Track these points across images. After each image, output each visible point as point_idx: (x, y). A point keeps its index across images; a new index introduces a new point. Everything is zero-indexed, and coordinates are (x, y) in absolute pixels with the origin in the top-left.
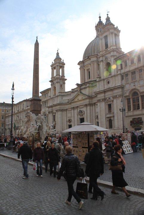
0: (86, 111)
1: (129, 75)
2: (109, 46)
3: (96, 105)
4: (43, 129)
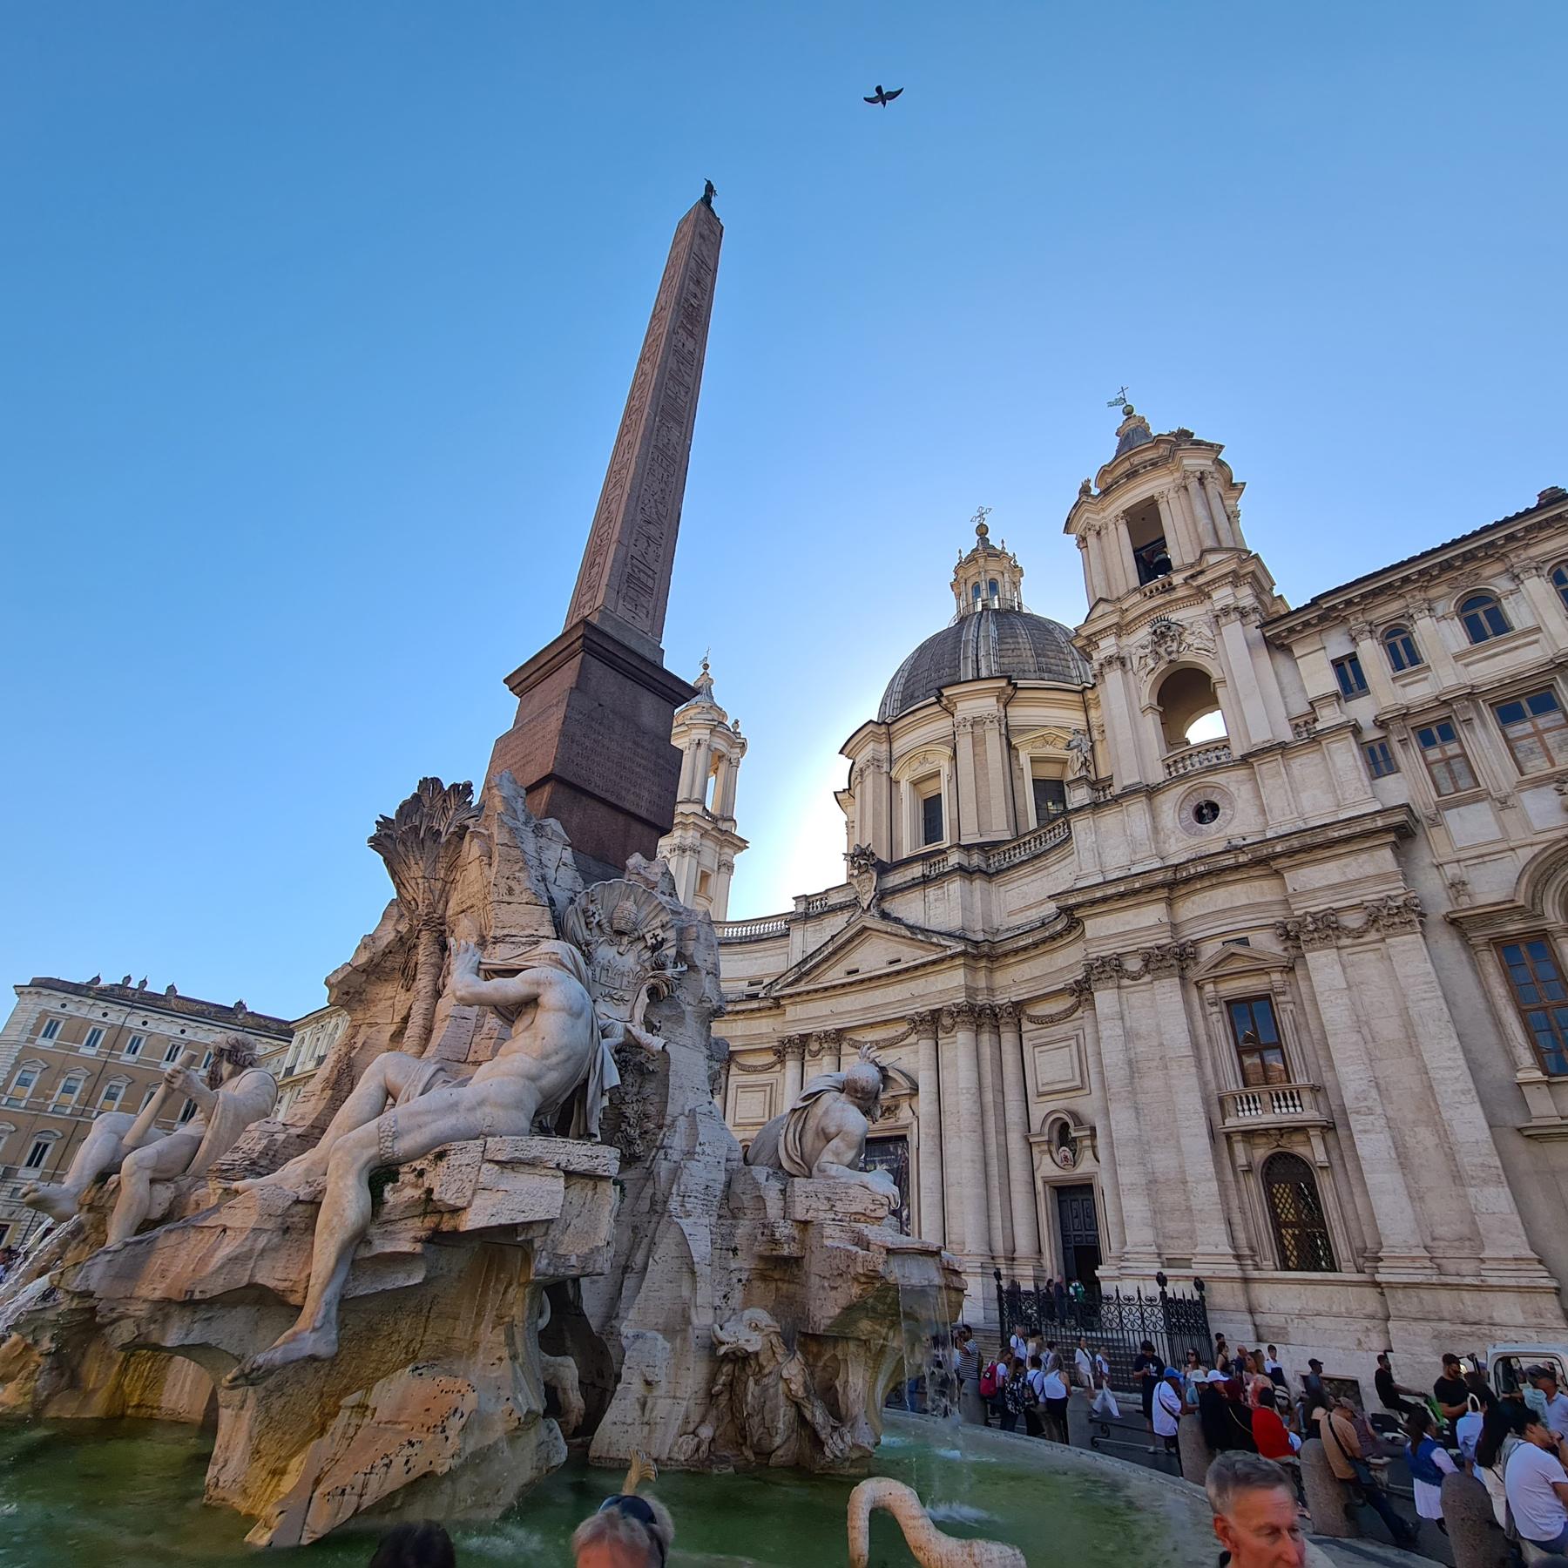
0: (934, 1073)
1: (1463, 733)
2: (1179, 550)
3: (1027, 1026)
4: (677, 1141)
